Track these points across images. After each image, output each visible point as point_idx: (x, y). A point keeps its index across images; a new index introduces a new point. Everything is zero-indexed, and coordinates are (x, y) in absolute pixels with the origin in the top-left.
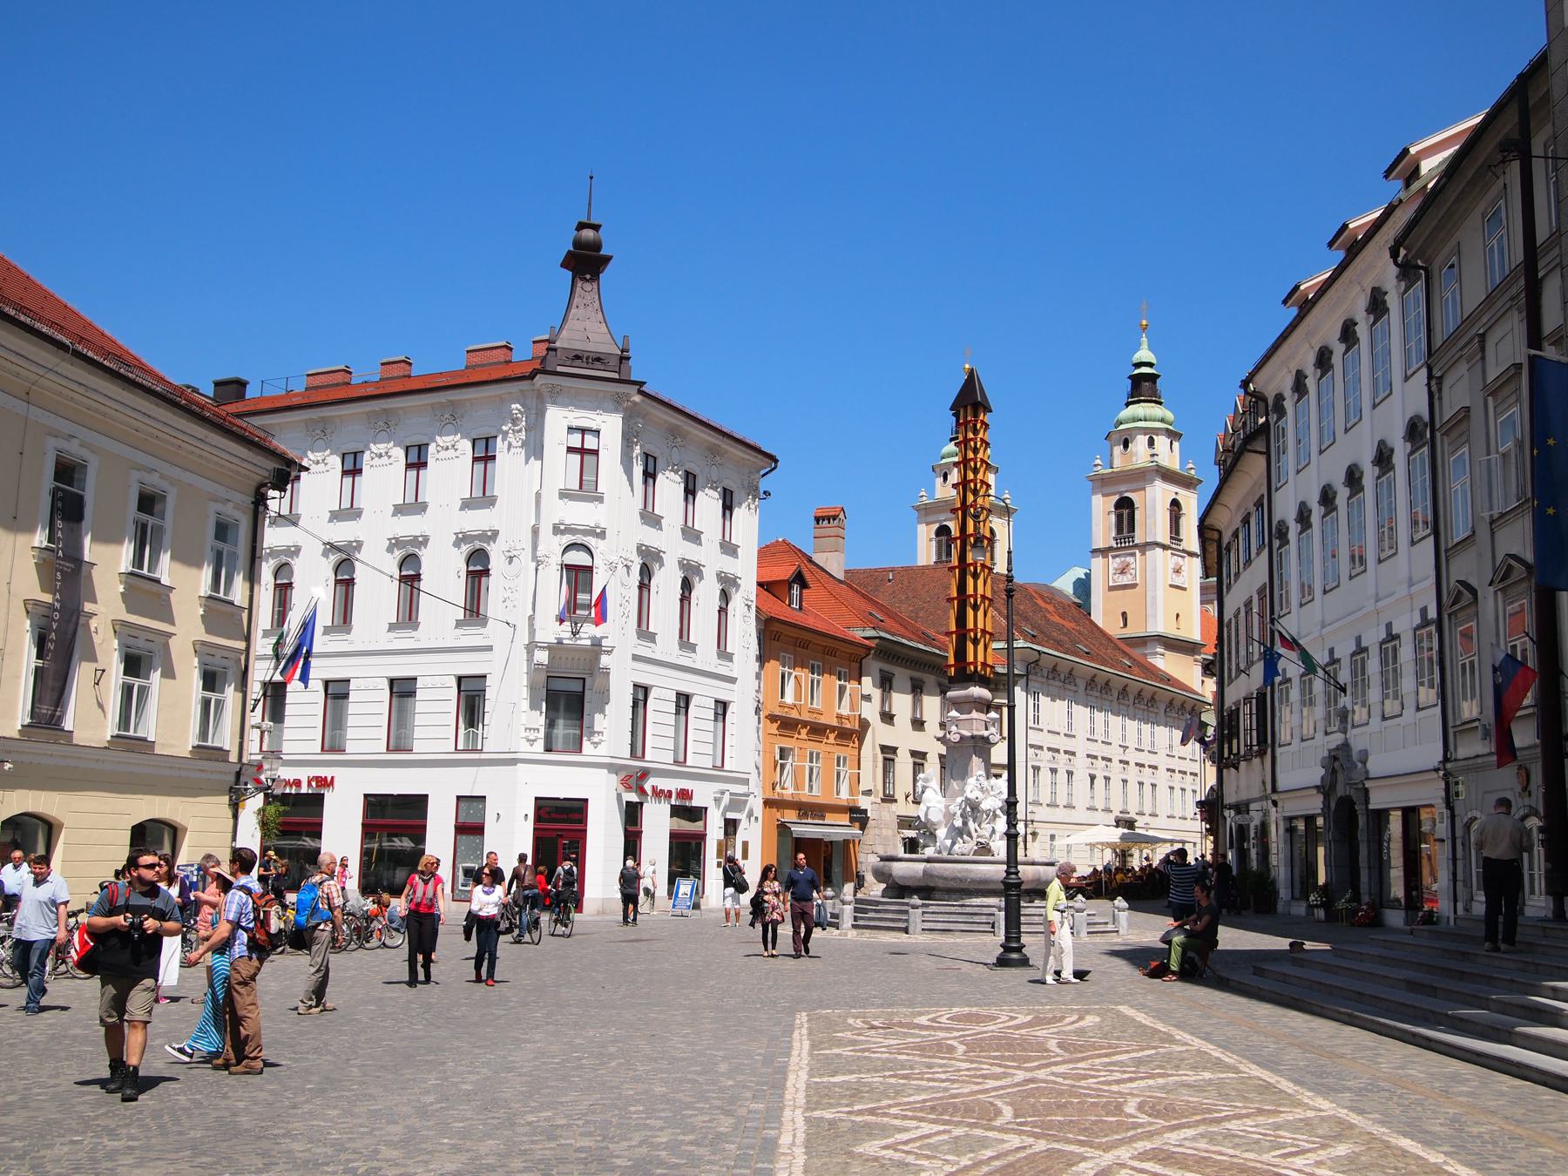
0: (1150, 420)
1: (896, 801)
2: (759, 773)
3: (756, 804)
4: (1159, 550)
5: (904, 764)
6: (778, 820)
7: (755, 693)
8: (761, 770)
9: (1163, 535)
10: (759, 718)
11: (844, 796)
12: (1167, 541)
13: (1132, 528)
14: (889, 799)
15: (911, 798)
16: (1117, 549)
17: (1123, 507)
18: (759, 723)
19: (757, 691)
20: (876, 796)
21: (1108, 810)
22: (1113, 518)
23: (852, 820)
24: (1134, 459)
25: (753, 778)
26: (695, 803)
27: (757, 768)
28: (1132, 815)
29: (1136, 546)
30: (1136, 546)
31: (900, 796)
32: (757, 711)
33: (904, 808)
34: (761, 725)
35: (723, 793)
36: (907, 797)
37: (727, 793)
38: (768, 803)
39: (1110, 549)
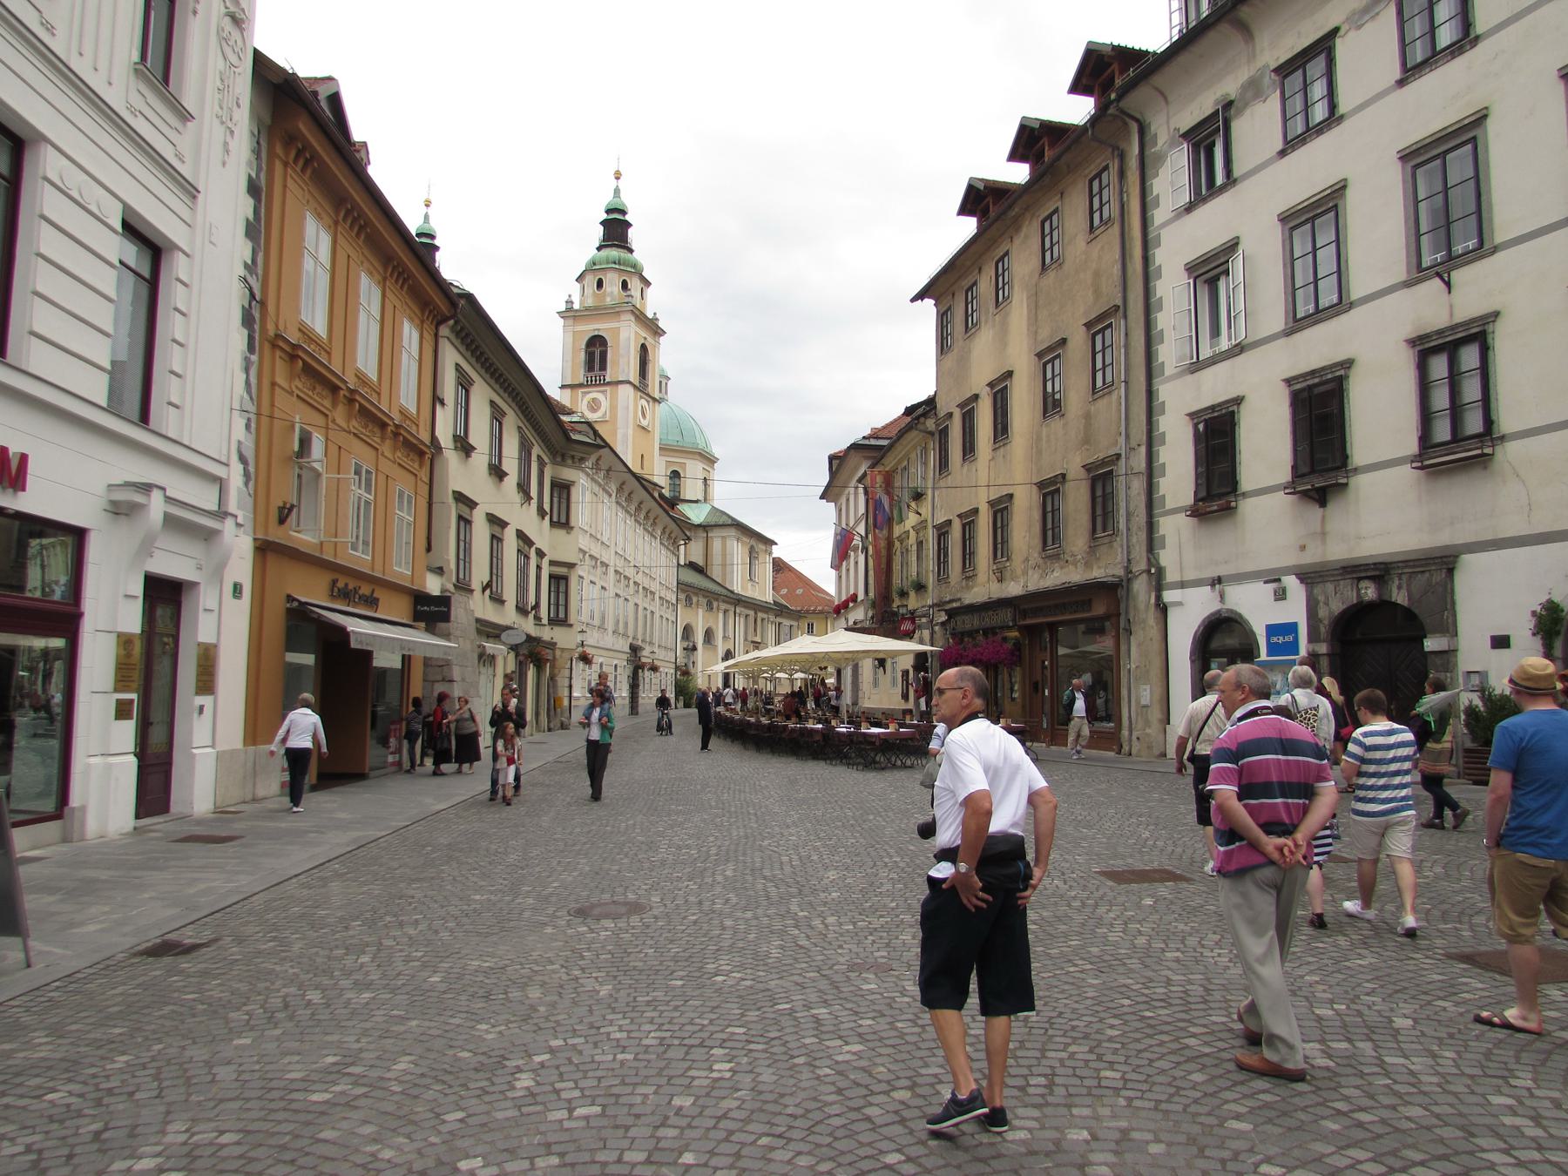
0: (624, 265)
1: (472, 591)
2: (246, 474)
3: (239, 546)
4: (628, 389)
5: (481, 533)
6: (290, 598)
7: (242, 271)
8: (252, 469)
9: (633, 375)
10: (251, 338)
11: (400, 569)
12: (637, 384)
13: (603, 367)
14: (464, 587)
15: (488, 592)
16: (587, 386)
17: (595, 346)
18: (251, 348)
19: (246, 266)
20: (449, 580)
21: (625, 635)
22: (582, 355)
23: (418, 616)
24: (608, 299)
25: (235, 476)
26: (31, 501)
27: (242, 459)
28: (640, 643)
29: (609, 383)
30: (609, 383)
31: (476, 585)
32: (248, 320)
33: (480, 606)
34: (254, 358)
35: (146, 488)
36: (484, 590)
37: (157, 496)
38: (265, 550)
39: (581, 386)
